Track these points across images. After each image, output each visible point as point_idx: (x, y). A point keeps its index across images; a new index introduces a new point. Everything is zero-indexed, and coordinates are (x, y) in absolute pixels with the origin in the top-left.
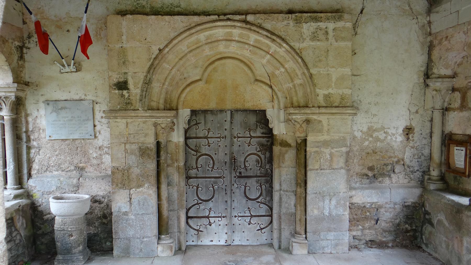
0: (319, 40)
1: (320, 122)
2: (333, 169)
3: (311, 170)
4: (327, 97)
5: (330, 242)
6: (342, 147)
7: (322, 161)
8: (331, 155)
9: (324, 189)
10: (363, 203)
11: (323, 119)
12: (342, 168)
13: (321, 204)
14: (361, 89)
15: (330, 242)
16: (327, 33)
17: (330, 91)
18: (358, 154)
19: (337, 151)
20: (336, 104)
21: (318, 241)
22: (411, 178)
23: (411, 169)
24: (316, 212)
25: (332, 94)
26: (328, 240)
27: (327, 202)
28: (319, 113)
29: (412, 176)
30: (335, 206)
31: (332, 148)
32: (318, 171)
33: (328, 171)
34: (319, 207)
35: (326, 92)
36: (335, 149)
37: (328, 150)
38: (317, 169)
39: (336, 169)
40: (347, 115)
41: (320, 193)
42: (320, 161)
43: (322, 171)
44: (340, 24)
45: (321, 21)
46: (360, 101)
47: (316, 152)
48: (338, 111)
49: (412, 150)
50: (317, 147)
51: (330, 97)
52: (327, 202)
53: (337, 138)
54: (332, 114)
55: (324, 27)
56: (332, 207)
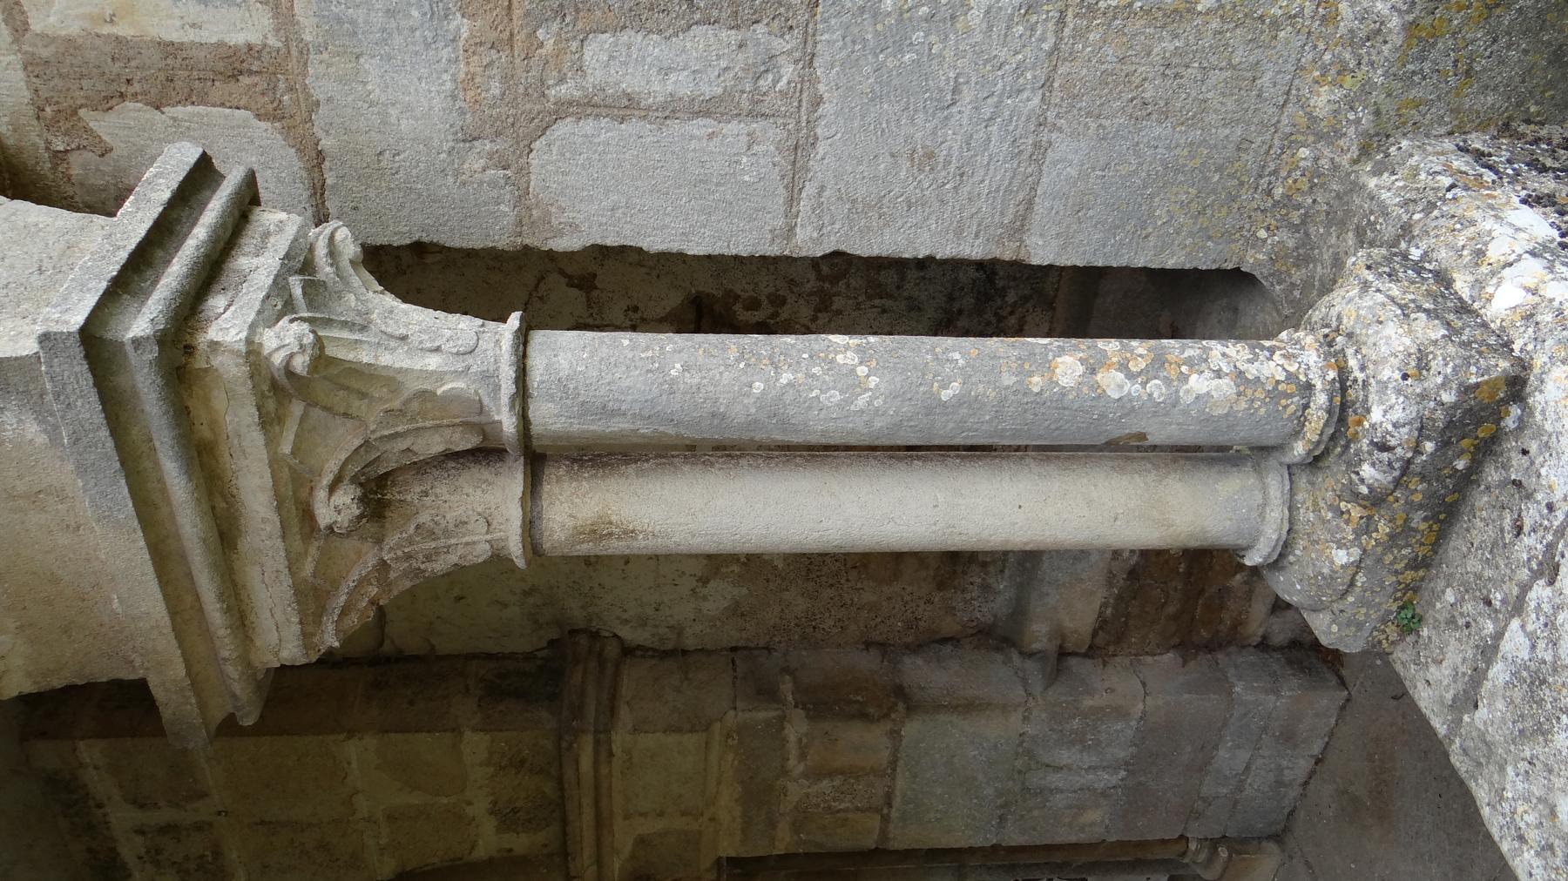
0: (217, 854)
1: (642, 841)
2: (894, 763)
3: (884, 833)
4: (508, 818)
5: (1260, 761)
6: (784, 740)
7: (843, 806)
8: (816, 774)
9: (989, 791)
10: (1110, 578)
11: (623, 838)
12: (895, 735)
13: (1059, 801)
14: (456, 592)
15: (1260, 761)
16: (167, 829)
17: (479, 807)
18: (830, 592)
19: (803, 756)
20: (549, 788)
21: (1236, 803)
22: (1025, 299)
23: (968, 301)
24: (1092, 816)
25: (495, 803)
26: (1247, 768)
27: (1055, 780)
28: (599, 861)
29: (1011, 297)
30: (1085, 748)
31: (784, 772)
32: (894, 814)
33: (901, 783)
34: (1070, 807)
35: (488, 826)
36: (792, 762)
37: (791, 786)
38: (886, 819)
39: (896, 751)
40: (604, 770)
41: (1006, 805)
42: (846, 810)
43: (897, 802)
44: (99, 783)
45: (112, 850)
46: (526, 594)
47: (796, 827)
48: (587, 802)
49: (838, 303)
50: (773, 825)
51: (514, 811)
52: (1055, 780)
53: (730, 757)
54: (600, 823)
55: (139, 839)
56: (1089, 759)
